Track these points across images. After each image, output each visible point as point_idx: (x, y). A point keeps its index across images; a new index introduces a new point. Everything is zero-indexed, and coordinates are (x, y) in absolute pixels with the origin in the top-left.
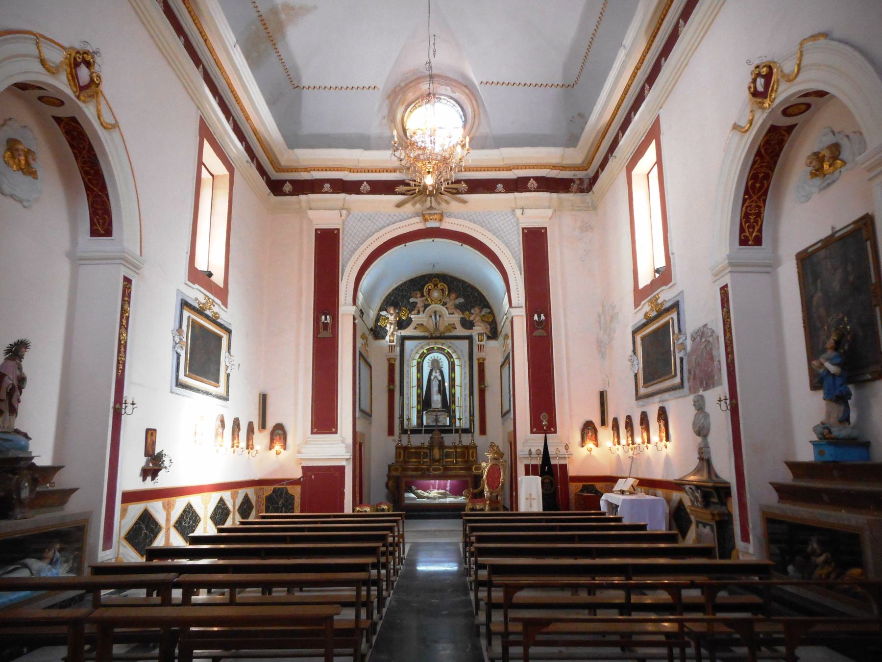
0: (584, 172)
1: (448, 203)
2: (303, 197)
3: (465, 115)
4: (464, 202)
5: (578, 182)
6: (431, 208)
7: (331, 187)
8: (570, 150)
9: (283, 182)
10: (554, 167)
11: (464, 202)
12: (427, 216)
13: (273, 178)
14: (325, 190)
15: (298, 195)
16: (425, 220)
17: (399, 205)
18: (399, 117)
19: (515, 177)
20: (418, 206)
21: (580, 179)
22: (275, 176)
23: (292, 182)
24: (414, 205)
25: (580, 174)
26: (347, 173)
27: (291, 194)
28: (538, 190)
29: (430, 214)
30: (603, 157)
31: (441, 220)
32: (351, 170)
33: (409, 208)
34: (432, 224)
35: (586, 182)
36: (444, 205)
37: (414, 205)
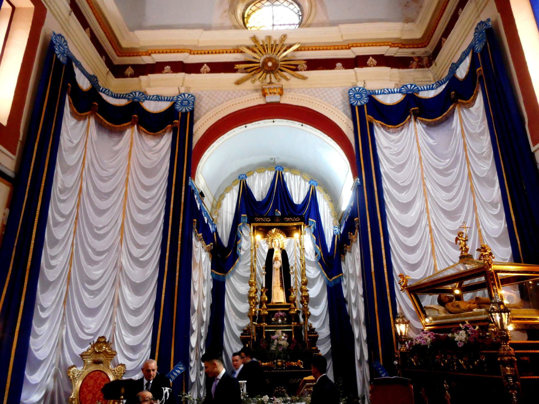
0: (423, 50)
1: (287, 79)
2: (143, 78)
3: (302, 10)
4: (304, 78)
5: (417, 60)
6: (271, 83)
7: (171, 69)
8: (409, 26)
9: (126, 66)
10: (393, 44)
11: (304, 78)
12: (267, 91)
13: (116, 63)
14: (166, 71)
15: (138, 76)
16: (264, 95)
17: (238, 83)
18: (239, 12)
19: (353, 56)
20: (258, 83)
21: (419, 57)
22: (118, 60)
23: (134, 66)
24: (253, 82)
25: (419, 52)
26: (186, 54)
27: (132, 76)
28: (378, 65)
29: (269, 88)
30: (437, 42)
31: (281, 94)
32: (191, 52)
33: (248, 84)
34: (271, 99)
35: (425, 60)
36: (283, 82)
37: (253, 82)
